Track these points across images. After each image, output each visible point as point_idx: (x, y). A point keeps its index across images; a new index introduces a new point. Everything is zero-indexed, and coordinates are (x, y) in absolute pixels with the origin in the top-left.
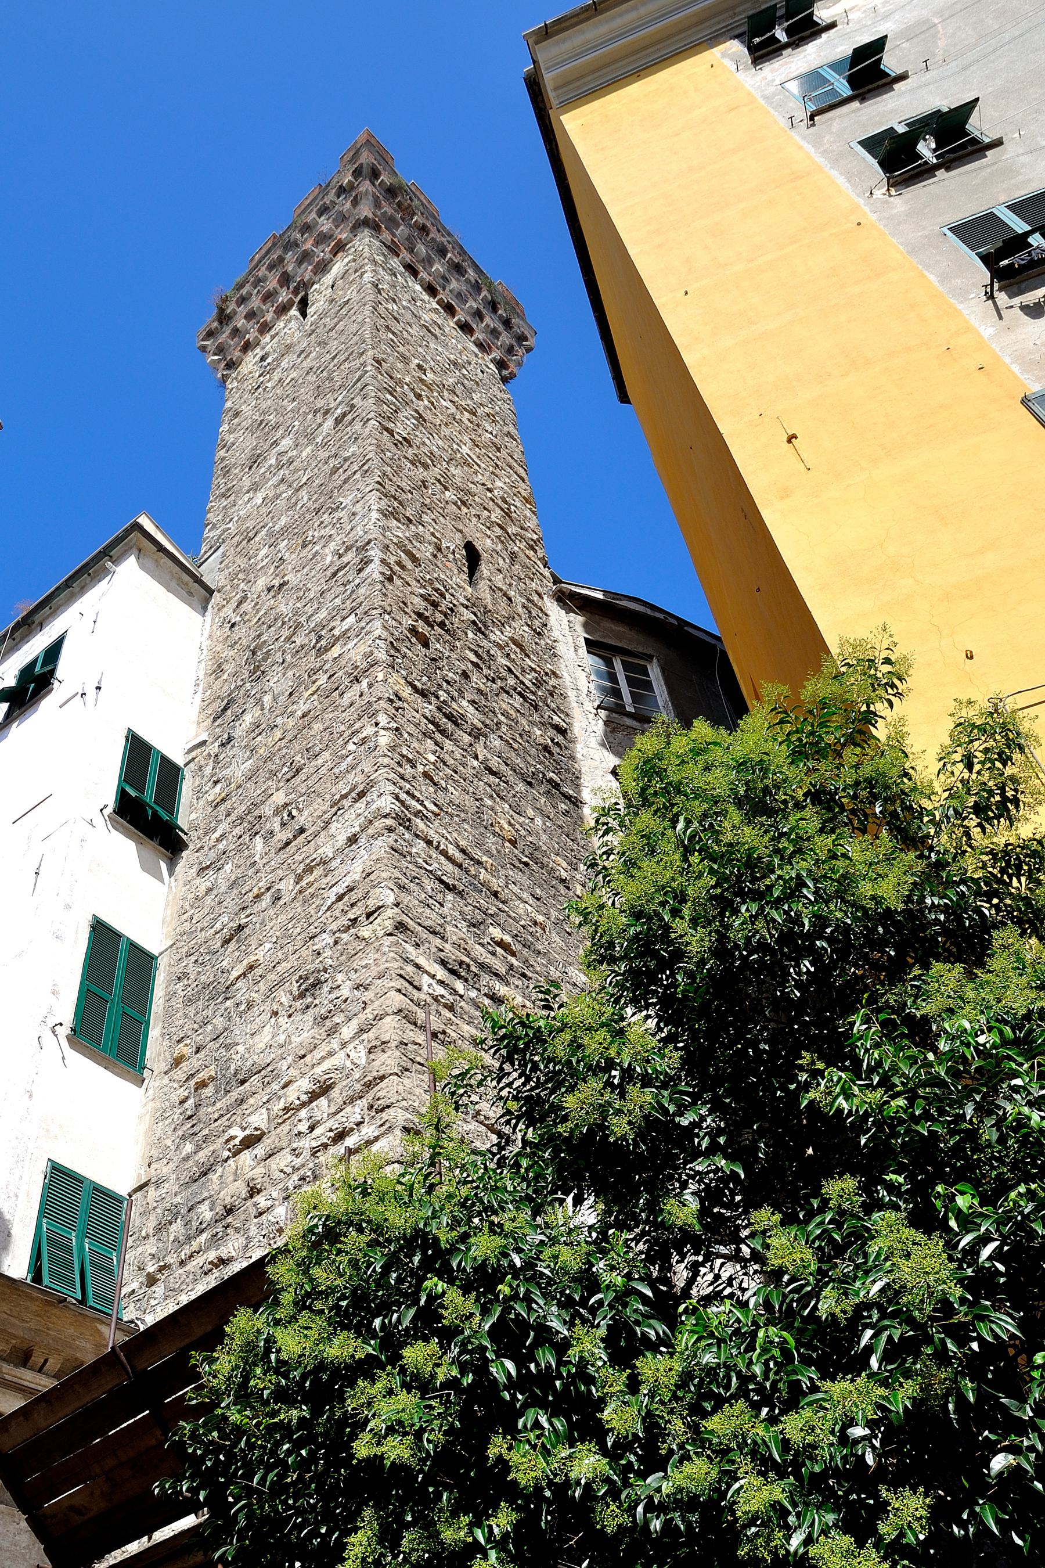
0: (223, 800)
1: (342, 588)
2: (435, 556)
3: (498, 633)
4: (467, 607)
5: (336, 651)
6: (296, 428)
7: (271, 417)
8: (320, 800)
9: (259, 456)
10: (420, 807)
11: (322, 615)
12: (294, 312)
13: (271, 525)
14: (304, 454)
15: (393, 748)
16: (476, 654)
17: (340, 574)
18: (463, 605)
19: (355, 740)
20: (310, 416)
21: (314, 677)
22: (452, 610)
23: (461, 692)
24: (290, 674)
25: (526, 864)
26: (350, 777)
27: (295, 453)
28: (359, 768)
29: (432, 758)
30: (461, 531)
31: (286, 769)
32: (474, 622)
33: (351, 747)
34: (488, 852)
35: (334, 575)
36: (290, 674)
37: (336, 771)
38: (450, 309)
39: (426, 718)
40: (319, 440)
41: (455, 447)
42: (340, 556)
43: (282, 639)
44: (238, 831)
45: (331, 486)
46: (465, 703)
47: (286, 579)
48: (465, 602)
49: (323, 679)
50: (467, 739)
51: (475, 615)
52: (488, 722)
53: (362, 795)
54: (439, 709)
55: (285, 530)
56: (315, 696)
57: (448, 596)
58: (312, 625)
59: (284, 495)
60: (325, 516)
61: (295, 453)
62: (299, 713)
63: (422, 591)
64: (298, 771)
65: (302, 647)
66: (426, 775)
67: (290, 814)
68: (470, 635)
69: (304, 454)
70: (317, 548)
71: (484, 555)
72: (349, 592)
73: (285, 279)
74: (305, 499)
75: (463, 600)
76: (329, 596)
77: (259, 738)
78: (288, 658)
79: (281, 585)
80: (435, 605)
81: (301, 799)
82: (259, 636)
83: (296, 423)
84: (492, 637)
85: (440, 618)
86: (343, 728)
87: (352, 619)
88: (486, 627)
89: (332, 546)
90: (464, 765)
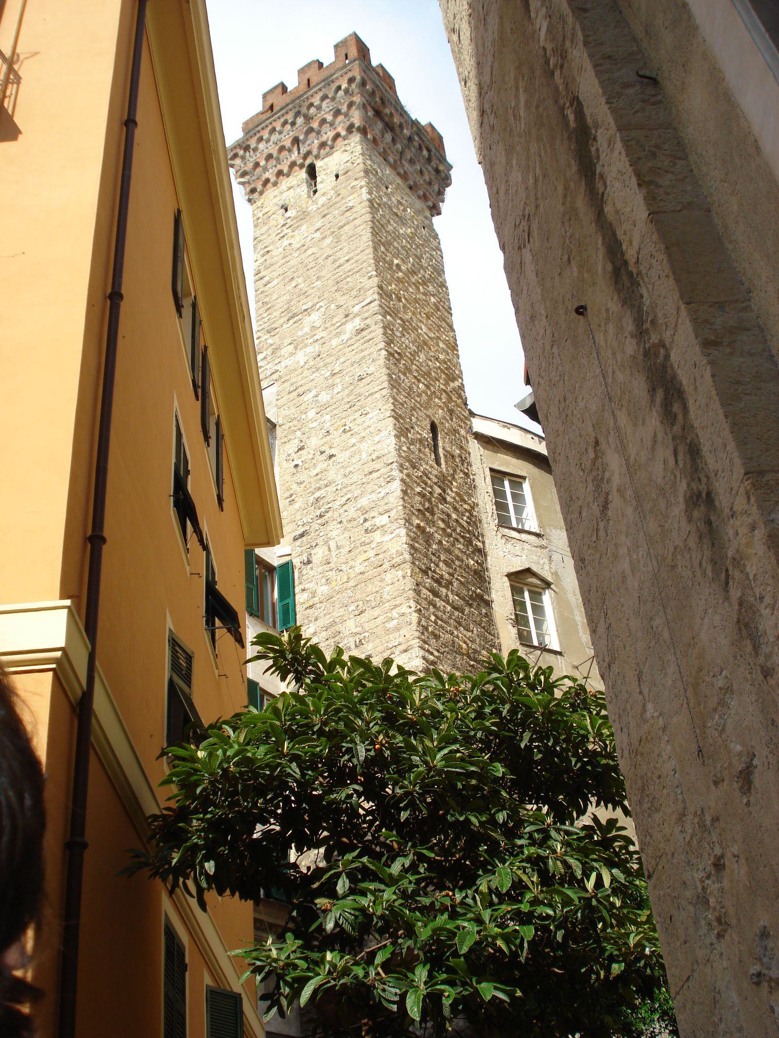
0: (311, 607)
1: (376, 487)
2: (420, 450)
3: (450, 493)
4: (436, 484)
5: (377, 536)
6: (323, 309)
7: (300, 280)
8: (378, 641)
9: (295, 315)
10: (431, 658)
11: (364, 502)
12: (303, 174)
13: (314, 393)
14: (335, 342)
15: (419, 623)
16: (443, 521)
17: (375, 475)
18: (436, 484)
19: (397, 610)
20: (333, 306)
21: (364, 548)
22: (430, 493)
23: (439, 557)
24: (346, 535)
25: (472, 666)
26: (396, 634)
27: (324, 334)
28: (401, 632)
29: (433, 618)
30: (428, 416)
31: (352, 608)
32: (440, 494)
33: (395, 614)
34: (458, 669)
35: (371, 473)
36: (346, 535)
37: (386, 625)
38: (404, 177)
39: (427, 589)
40: (345, 337)
41: (420, 331)
42: (373, 460)
43: (338, 503)
44: (324, 634)
45: (357, 391)
46: (441, 564)
47: (333, 452)
48: (436, 480)
49: (371, 554)
50: (444, 590)
51: (439, 487)
52: (451, 571)
53: (405, 651)
54: (432, 578)
55: (326, 406)
56: (366, 563)
57: (429, 482)
58: (359, 506)
59: (323, 372)
60: (357, 415)
61: (324, 334)
62: (357, 570)
63: (418, 489)
64: (362, 612)
65: (355, 520)
66: (432, 633)
67: (360, 641)
68: (440, 506)
69: (335, 342)
70: (353, 440)
71: (438, 425)
72: (382, 494)
73: (296, 141)
74: (340, 387)
75: (436, 480)
76: (369, 488)
77: (330, 573)
78: (344, 520)
79: (331, 456)
80: (423, 496)
81: (366, 634)
82: (319, 489)
83: (322, 304)
84: (448, 499)
85: (427, 505)
86: (388, 598)
87: (386, 516)
88: (444, 491)
89: (364, 446)
90: (444, 612)
